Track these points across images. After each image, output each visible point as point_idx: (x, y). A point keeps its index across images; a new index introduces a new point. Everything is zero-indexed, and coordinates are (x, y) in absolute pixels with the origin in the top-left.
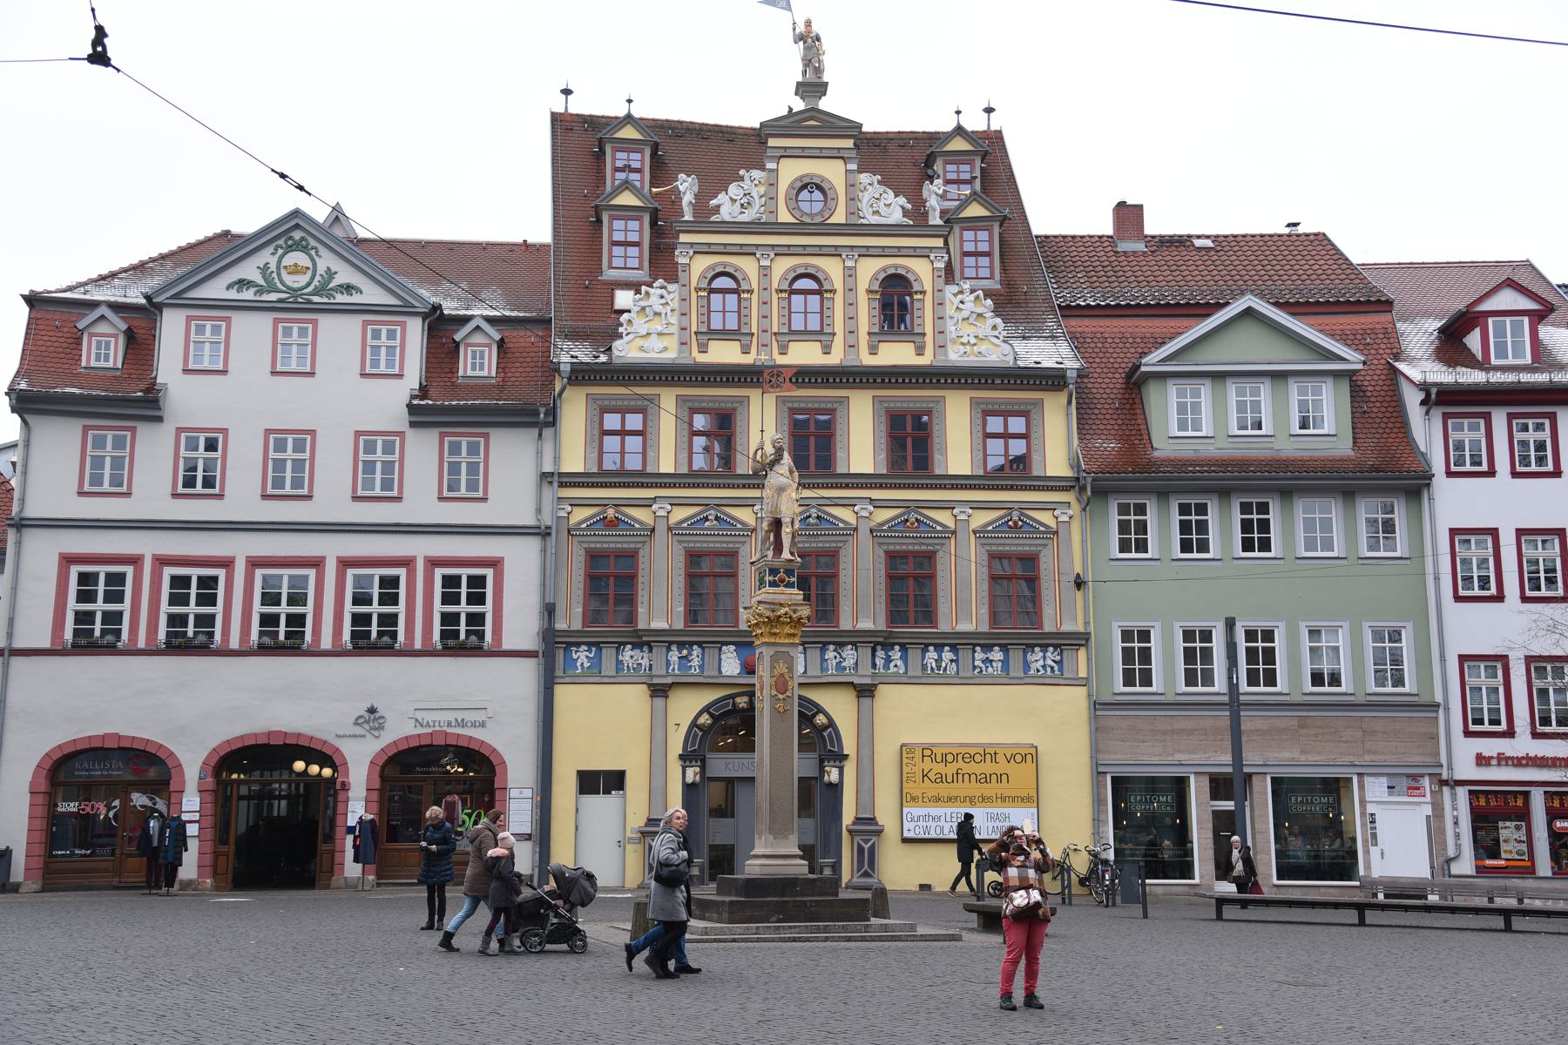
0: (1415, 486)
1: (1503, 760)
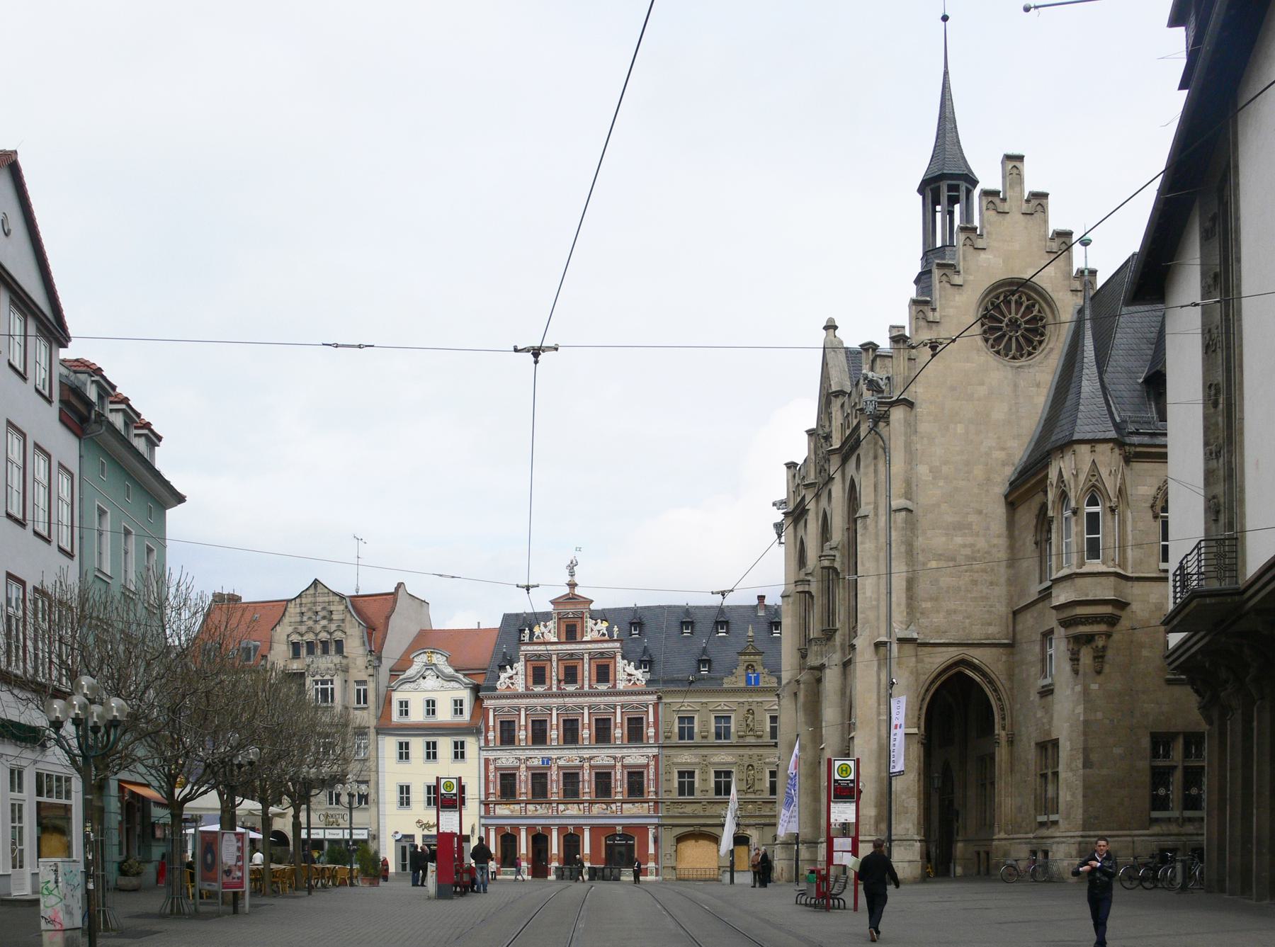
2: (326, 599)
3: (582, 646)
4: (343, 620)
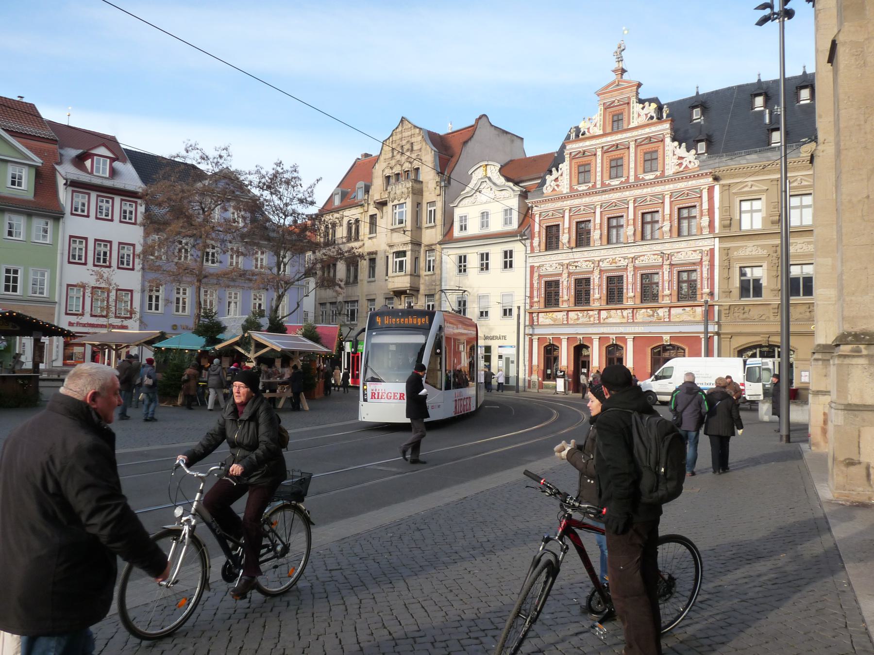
0: (57, 215)
1: (78, 324)
2: (409, 133)
3: (629, 134)
4: (420, 150)
